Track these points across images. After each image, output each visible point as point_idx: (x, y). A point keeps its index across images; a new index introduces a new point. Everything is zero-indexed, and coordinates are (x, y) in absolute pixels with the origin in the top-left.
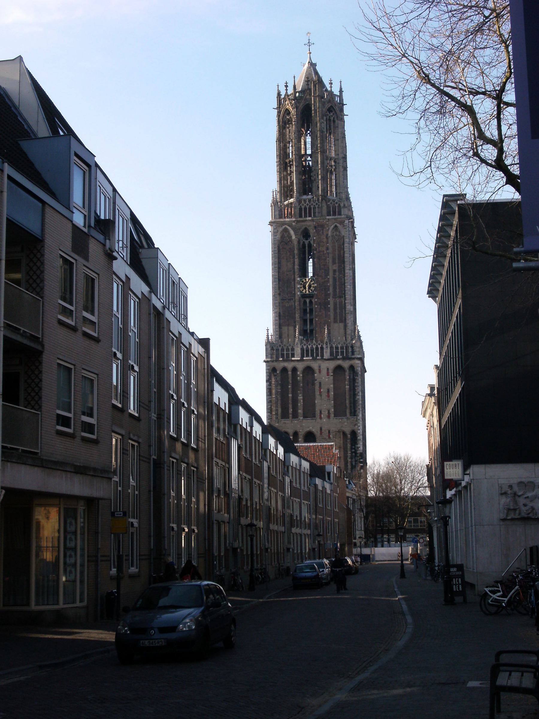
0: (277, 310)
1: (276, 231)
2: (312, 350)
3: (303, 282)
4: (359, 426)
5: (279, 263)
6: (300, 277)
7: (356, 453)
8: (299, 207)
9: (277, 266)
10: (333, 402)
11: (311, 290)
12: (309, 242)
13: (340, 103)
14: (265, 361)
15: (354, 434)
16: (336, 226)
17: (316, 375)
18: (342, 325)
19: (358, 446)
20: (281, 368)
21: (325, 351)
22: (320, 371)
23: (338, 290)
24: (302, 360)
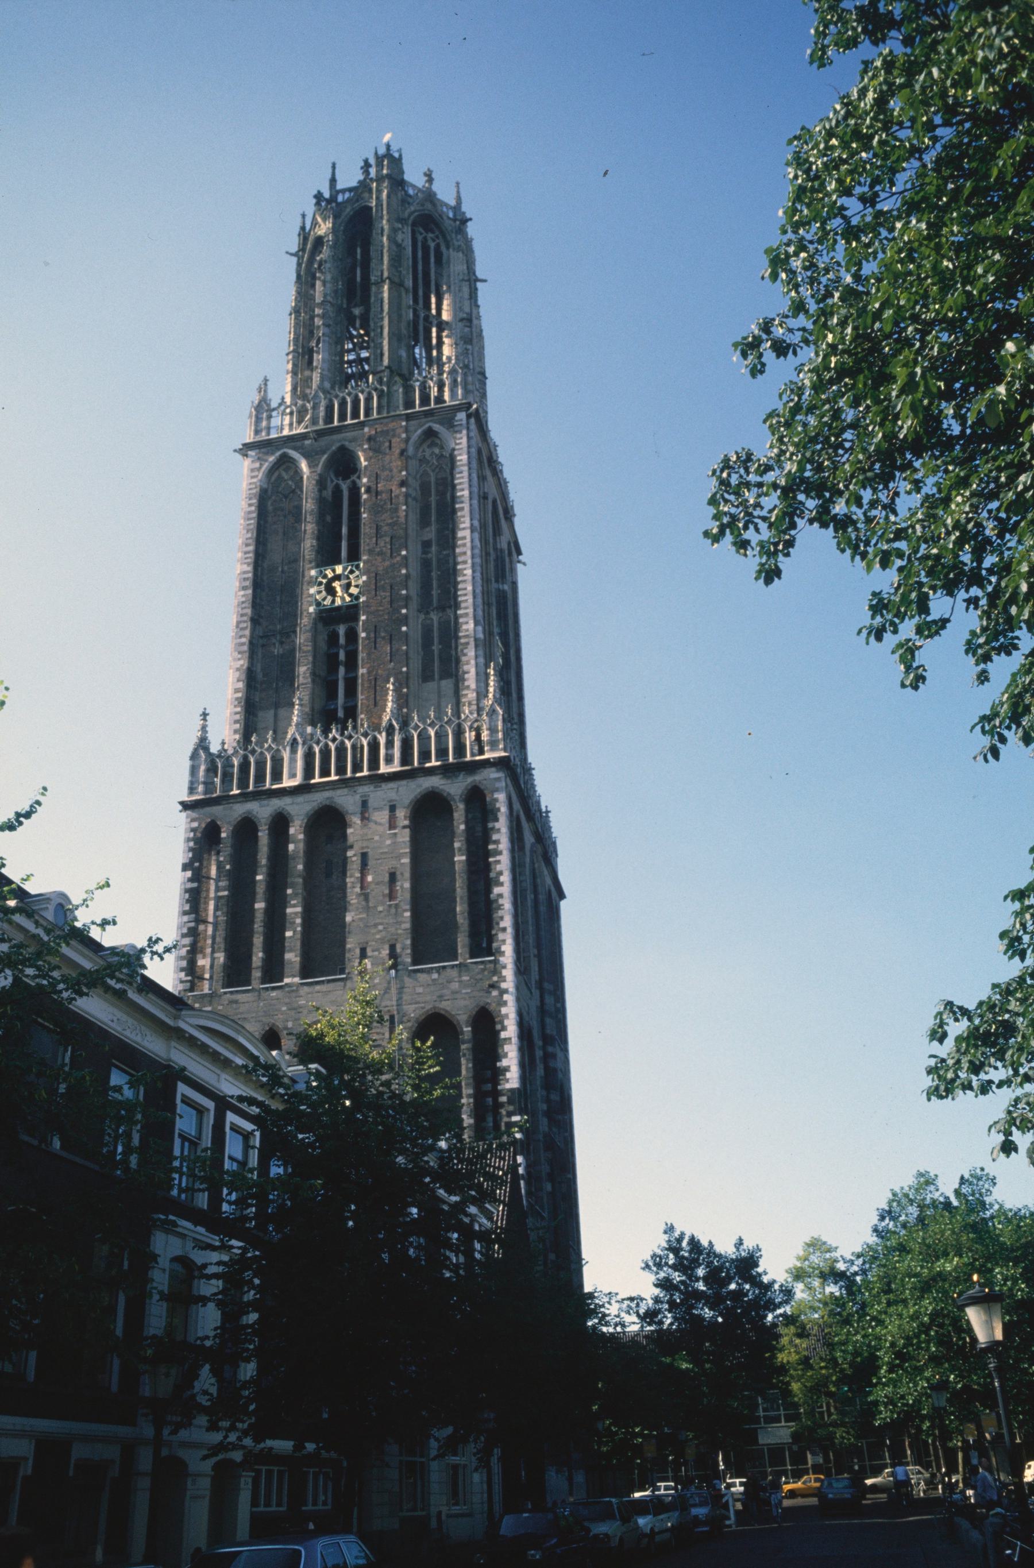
0: (243, 663)
3: (325, 576)
6: (317, 566)
7: (496, 1093)
9: (251, 548)
10: (408, 914)
11: (350, 595)
12: (354, 482)
13: (455, 220)
14: (186, 806)
15: (486, 1022)
17: (349, 831)
19: (504, 1063)
21: (382, 751)
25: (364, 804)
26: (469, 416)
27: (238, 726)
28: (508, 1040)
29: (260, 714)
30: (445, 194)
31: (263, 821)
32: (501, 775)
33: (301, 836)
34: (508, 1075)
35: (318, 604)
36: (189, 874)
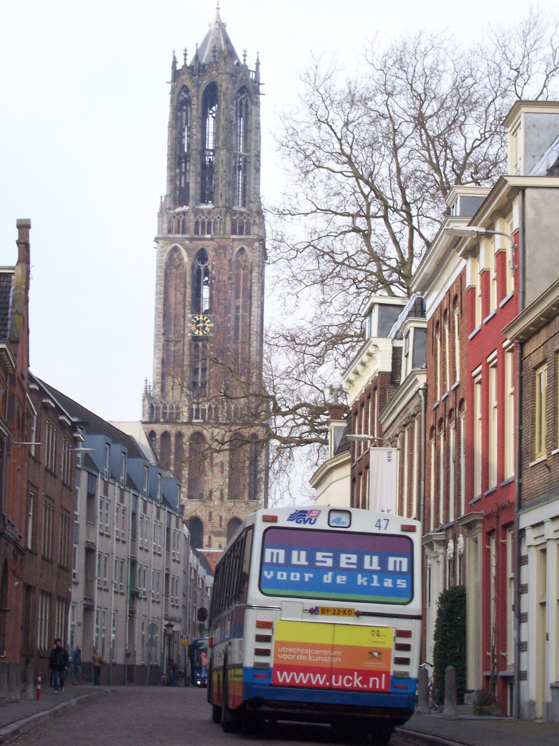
0: (160, 355)
1: (163, 250)
3: (195, 319)
5: (166, 292)
6: (192, 313)
8: (194, 220)
9: (162, 296)
12: (206, 267)
16: (242, 249)
24: (189, 423)
29: (166, 378)
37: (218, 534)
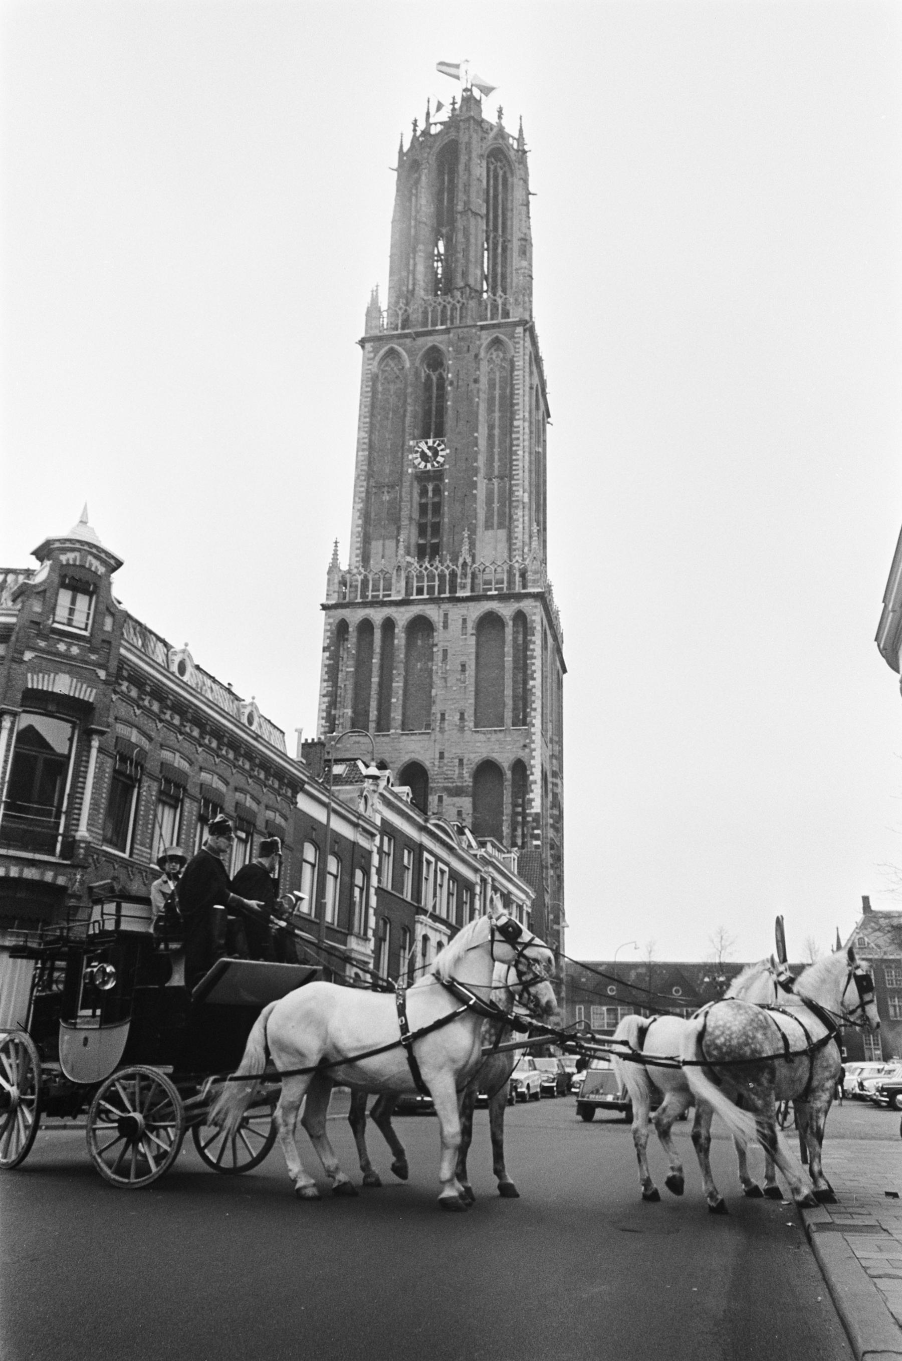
2: (431, 589)
4: (534, 750)
7: (524, 815)
11: (438, 462)
13: (518, 151)
14: (324, 607)
15: (520, 768)
18: (502, 534)
19: (531, 796)
20: (357, 622)
22: (445, 627)
23: (496, 464)
25: (446, 615)
26: (525, 330)
27: (358, 551)
28: (535, 782)
29: (374, 543)
30: (511, 129)
31: (378, 622)
32: (538, 604)
33: (403, 635)
34: (533, 804)
35: (415, 467)
36: (327, 654)
37: (457, 792)
